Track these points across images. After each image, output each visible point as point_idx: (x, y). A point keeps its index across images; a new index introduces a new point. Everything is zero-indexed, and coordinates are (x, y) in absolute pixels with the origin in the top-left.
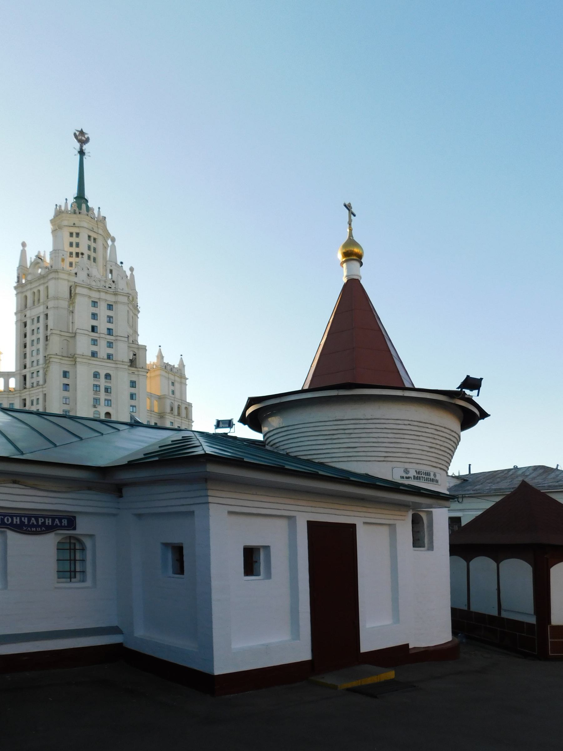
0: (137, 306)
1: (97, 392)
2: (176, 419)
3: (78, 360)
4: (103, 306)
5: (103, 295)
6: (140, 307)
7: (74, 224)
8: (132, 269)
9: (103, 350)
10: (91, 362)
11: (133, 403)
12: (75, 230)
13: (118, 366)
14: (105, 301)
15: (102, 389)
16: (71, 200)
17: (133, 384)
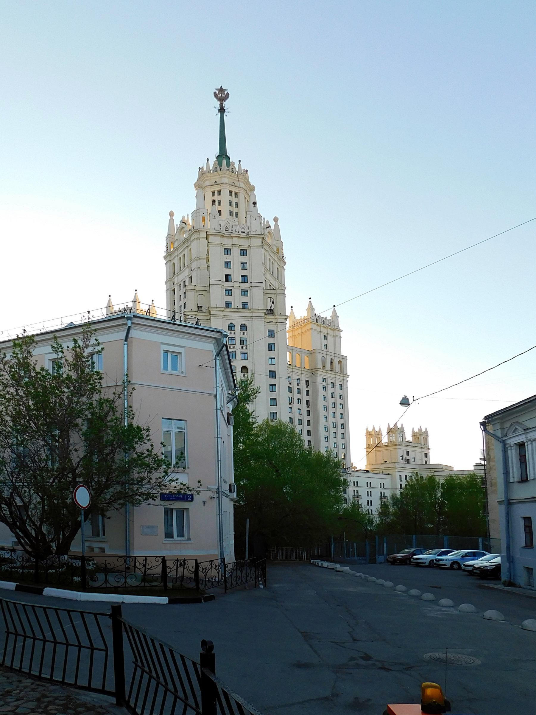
0: (283, 257)
1: (233, 345)
2: (329, 375)
3: (212, 313)
4: (236, 252)
5: (236, 241)
6: (285, 258)
7: (216, 182)
8: (276, 220)
9: (237, 299)
10: (225, 313)
11: (272, 354)
12: (216, 188)
13: (254, 314)
14: (238, 247)
15: (238, 342)
16: (213, 160)
17: (271, 334)
